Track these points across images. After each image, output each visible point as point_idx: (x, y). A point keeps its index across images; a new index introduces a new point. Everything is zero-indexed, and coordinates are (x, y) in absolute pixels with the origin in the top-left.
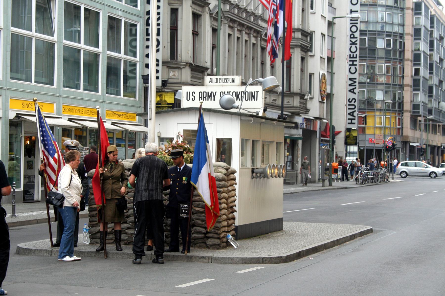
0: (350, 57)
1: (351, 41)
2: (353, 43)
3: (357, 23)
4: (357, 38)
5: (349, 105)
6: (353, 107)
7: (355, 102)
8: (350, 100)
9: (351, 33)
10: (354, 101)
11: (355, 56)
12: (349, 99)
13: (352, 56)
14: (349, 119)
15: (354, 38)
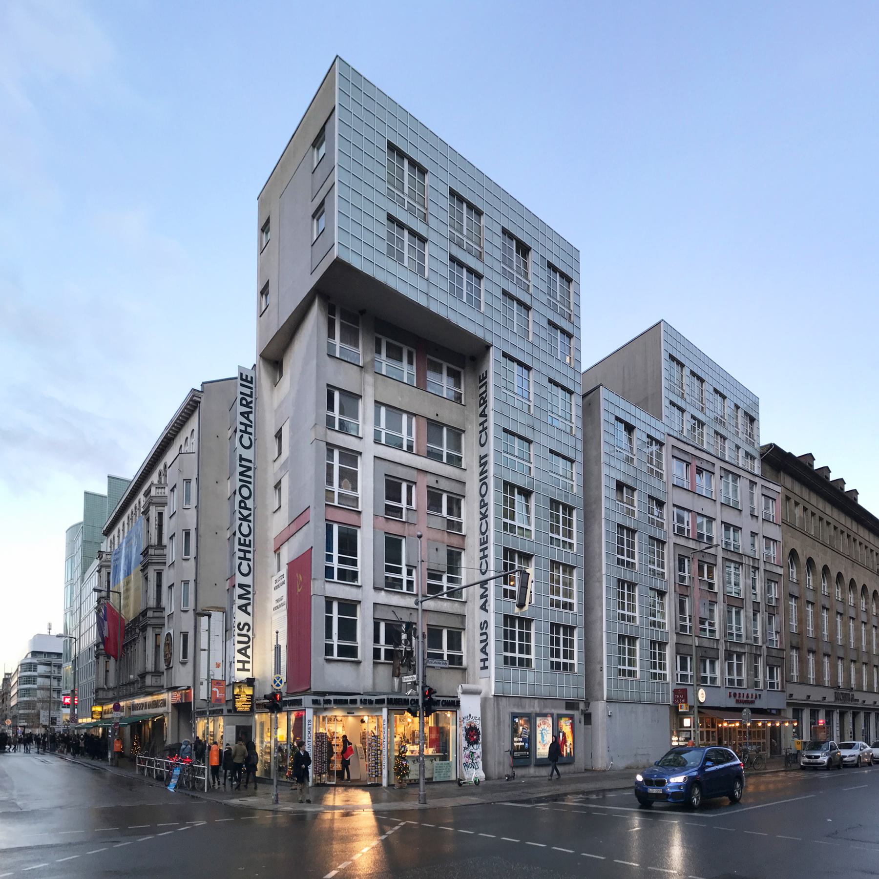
0: (240, 544)
1: (240, 512)
2: (245, 519)
3: (250, 483)
4: (250, 509)
5: (239, 635)
6: (246, 639)
7: (248, 631)
8: (241, 627)
9: (241, 499)
10: (246, 627)
11: (247, 543)
12: (239, 624)
13: (242, 542)
14: (239, 661)
15: (246, 508)
